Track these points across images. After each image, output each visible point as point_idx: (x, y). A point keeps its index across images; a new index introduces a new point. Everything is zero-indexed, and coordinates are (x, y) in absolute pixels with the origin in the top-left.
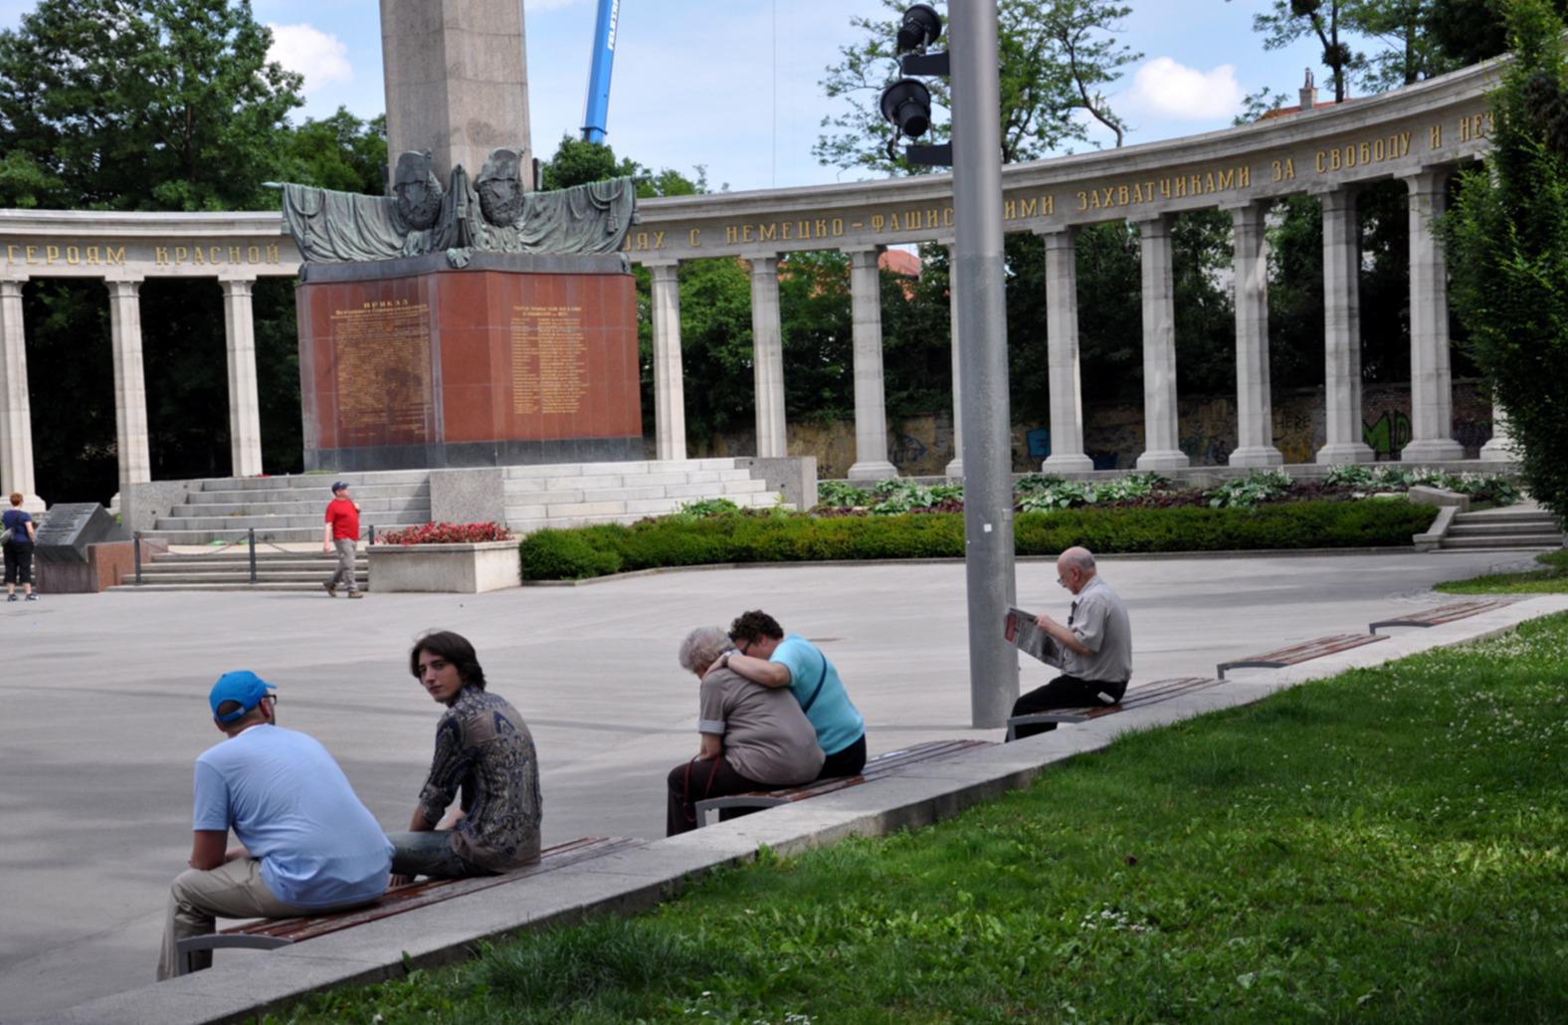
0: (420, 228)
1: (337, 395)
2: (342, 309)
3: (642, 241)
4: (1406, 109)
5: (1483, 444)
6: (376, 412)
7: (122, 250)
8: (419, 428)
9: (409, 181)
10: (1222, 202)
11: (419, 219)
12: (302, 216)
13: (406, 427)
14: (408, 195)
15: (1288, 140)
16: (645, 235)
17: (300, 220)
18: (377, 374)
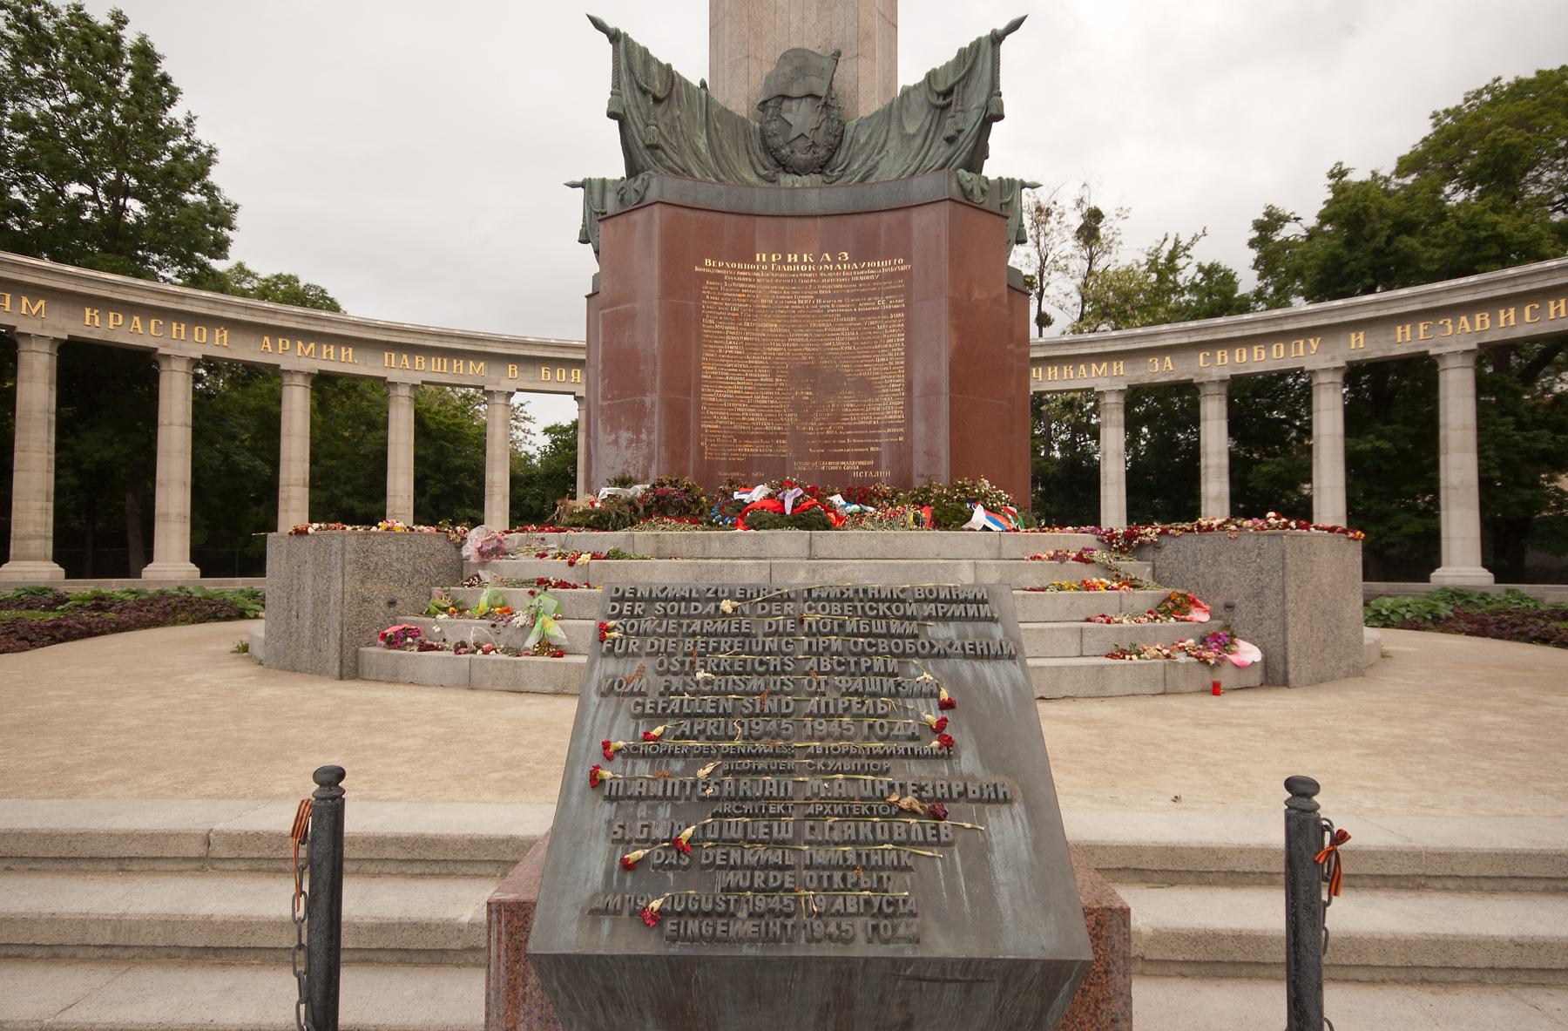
0: (799, 171)
1: (699, 403)
2: (716, 257)
3: (576, 375)
4: (1438, 300)
5: (1433, 571)
6: (766, 436)
7: (42, 303)
8: (863, 468)
9: (794, 92)
10: (1097, 385)
11: (801, 156)
12: (645, 92)
13: (833, 466)
14: (788, 117)
15: (1185, 340)
16: (579, 371)
17: (638, 94)
18: (773, 374)
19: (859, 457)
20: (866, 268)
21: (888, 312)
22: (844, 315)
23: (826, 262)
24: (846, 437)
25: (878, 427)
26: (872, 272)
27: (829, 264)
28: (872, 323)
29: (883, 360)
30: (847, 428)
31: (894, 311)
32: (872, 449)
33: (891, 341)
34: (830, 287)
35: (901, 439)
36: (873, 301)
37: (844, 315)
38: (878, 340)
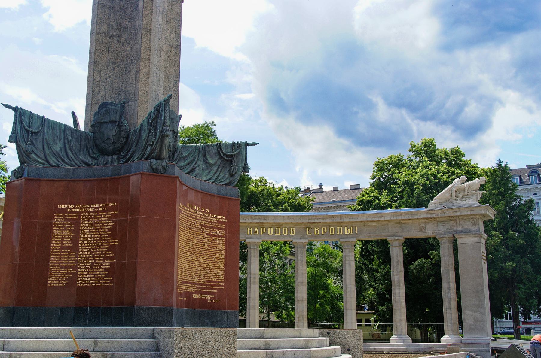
8: (211, 298)
19: (209, 293)
20: (213, 217)
21: (220, 236)
22: (207, 234)
23: (202, 212)
24: (206, 285)
25: (215, 282)
26: (216, 219)
27: (204, 212)
28: (215, 240)
29: (218, 255)
30: (207, 281)
31: (222, 236)
32: (214, 291)
33: (220, 248)
34: (204, 222)
35: (223, 288)
36: (215, 231)
37: (207, 234)
38: (216, 247)
